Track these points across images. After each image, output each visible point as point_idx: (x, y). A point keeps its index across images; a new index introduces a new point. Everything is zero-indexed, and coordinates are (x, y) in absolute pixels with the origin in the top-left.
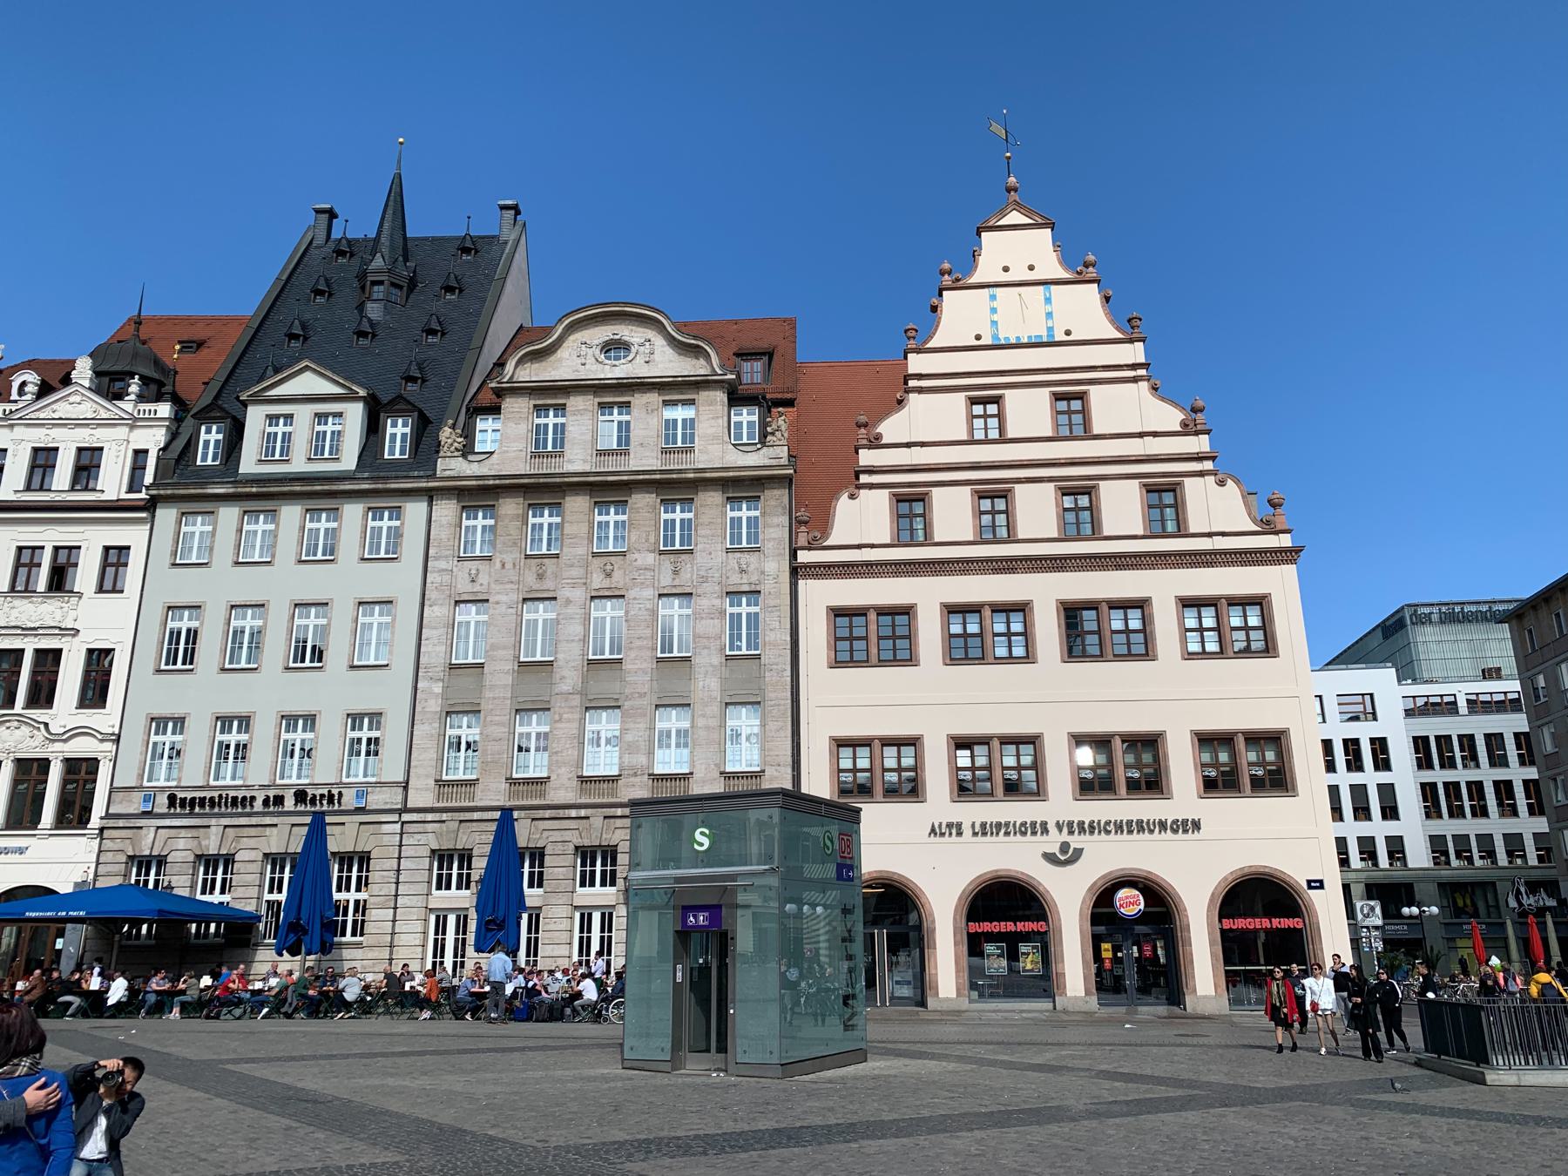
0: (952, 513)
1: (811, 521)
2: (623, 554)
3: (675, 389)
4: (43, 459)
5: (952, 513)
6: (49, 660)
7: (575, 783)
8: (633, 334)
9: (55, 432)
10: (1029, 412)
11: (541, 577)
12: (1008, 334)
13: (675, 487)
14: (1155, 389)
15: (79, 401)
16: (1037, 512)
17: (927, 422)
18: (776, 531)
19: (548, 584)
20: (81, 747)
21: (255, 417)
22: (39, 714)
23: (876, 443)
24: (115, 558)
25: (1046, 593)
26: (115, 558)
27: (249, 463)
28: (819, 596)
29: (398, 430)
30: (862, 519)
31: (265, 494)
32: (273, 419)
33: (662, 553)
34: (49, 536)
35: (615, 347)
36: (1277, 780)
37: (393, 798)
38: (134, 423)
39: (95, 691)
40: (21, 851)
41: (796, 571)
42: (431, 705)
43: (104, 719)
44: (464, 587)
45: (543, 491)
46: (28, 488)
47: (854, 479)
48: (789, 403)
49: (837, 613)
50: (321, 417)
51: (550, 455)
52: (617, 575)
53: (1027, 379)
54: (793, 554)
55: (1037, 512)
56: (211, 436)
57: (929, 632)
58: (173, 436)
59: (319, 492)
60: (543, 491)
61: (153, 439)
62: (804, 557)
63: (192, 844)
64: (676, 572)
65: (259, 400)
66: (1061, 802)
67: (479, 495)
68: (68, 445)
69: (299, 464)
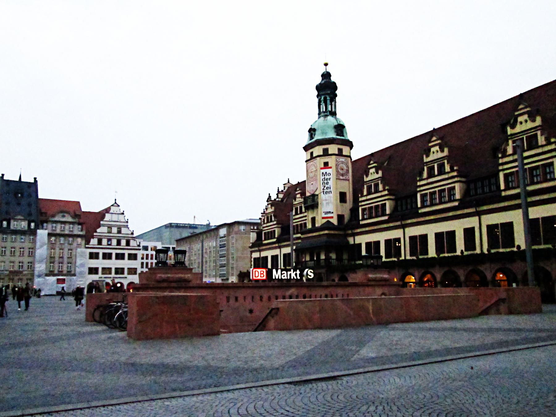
1: (88, 242)
5: (105, 242)
8: (65, 214)
10: (115, 230)
12: (114, 220)
16: (114, 242)
17: (102, 230)
18: (83, 242)
23: (96, 232)
25: (114, 252)
27: (12, 227)
29: (33, 225)
30: (94, 242)
31: (15, 232)
35: (64, 216)
36: (135, 273)
47: (93, 237)
53: (115, 226)
62: (87, 246)
66: (113, 275)
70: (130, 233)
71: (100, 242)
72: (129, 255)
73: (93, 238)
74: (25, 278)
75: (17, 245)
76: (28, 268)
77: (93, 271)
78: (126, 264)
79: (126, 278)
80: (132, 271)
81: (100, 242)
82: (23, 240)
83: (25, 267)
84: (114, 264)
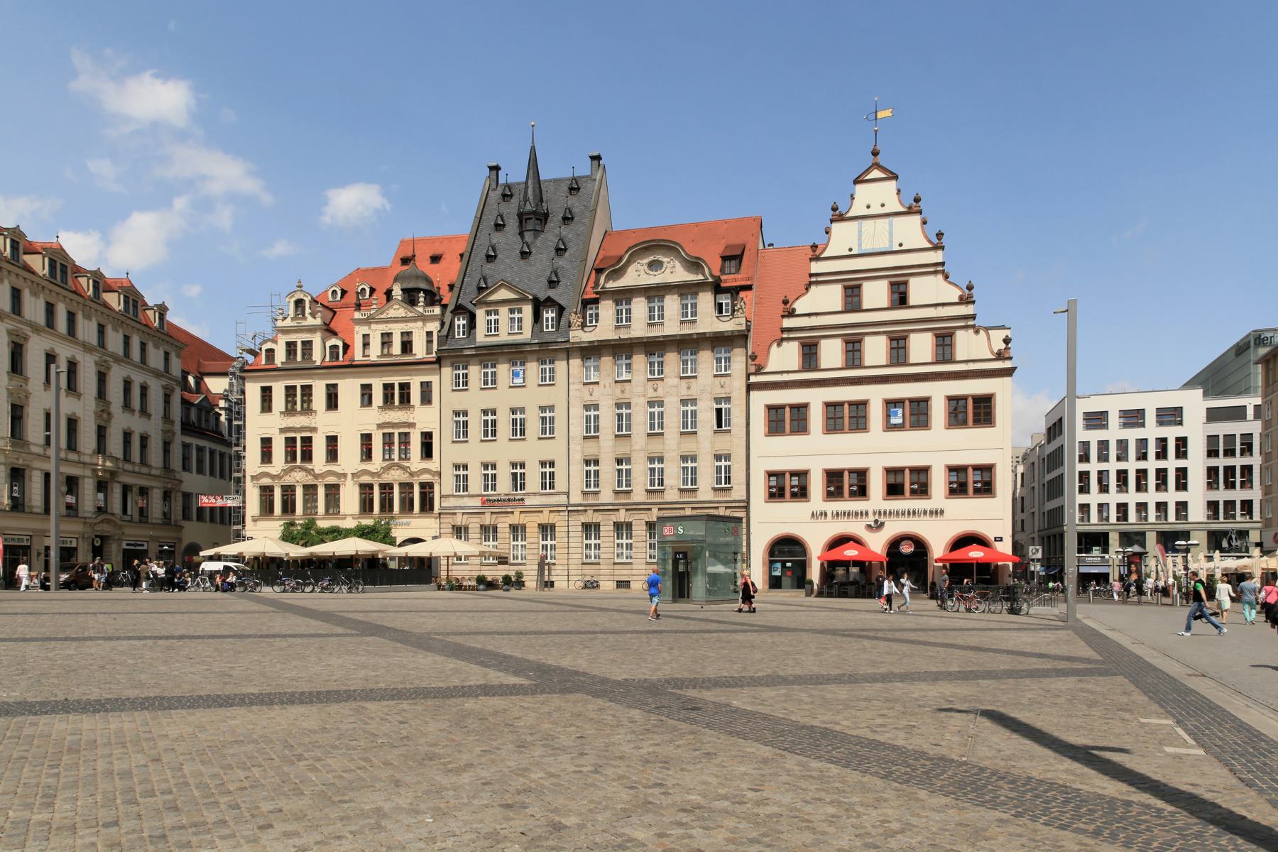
0: (831, 353)
2: (662, 379)
3: (686, 290)
4: (386, 339)
5: (831, 353)
6: (405, 439)
7: (644, 493)
9: (390, 326)
10: (876, 294)
11: (623, 392)
13: (687, 344)
14: (946, 277)
15: (397, 311)
16: (876, 350)
19: (627, 395)
20: (426, 478)
21: (480, 314)
22: (405, 463)
23: (791, 314)
24: (426, 388)
26: (426, 388)
27: (481, 336)
28: (761, 399)
31: (490, 354)
32: (489, 313)
33: (682, 378)
34: (396, 380)
35: (655, 265)
37: (562, 499)
38: (424, 319)
39: (427, 451)
40: (408, 524)
41: (750, 387)
42: (577, 457)
43: (433, 465)
44: (588, 399)
45: (621, 349)
46: (383, 355)
48: (749, 288)
49: (770, 408)
50: (512, 311)
51: (625, 327)
52: (660, 392)
54: (748, 378)
55: (876, 350)
56: (461, 322)
57: (816, 417)
58: (443, 324)
59: (515, 353)
60: (621, 349)
61: (434, 327)
62: (753, 379)
63: (477, 520)
64: (689, 388)
65: (481, 303)
67: (591, 351)
68: (397, 330)
69: (504, 337)
70: (953, 294)
71: (810, 353)
72: (955, 402)
73: (780, 342)
74: (532, 522)
75: (502, 399)
76: (544, 486)
77: (789, 486)
78: (941, 446)
79: (939, 513)
80: (972, 481)
81: (810, 353)
82: (519, 381)
83: (533, 482)
84: (876, 450)
